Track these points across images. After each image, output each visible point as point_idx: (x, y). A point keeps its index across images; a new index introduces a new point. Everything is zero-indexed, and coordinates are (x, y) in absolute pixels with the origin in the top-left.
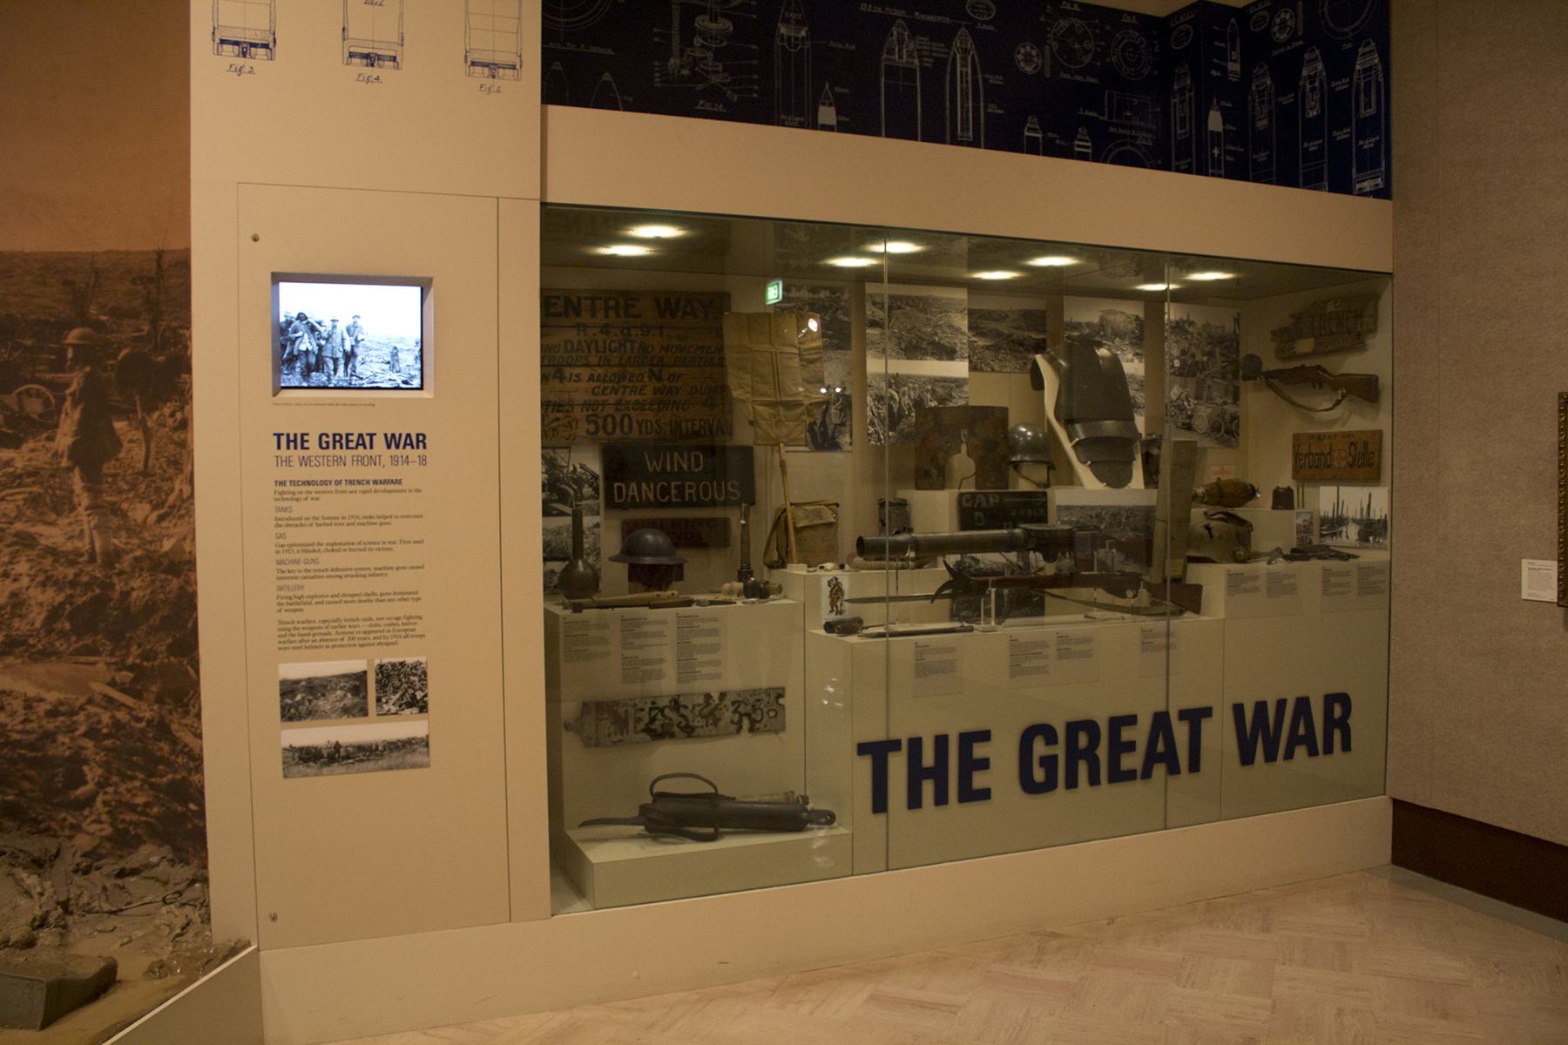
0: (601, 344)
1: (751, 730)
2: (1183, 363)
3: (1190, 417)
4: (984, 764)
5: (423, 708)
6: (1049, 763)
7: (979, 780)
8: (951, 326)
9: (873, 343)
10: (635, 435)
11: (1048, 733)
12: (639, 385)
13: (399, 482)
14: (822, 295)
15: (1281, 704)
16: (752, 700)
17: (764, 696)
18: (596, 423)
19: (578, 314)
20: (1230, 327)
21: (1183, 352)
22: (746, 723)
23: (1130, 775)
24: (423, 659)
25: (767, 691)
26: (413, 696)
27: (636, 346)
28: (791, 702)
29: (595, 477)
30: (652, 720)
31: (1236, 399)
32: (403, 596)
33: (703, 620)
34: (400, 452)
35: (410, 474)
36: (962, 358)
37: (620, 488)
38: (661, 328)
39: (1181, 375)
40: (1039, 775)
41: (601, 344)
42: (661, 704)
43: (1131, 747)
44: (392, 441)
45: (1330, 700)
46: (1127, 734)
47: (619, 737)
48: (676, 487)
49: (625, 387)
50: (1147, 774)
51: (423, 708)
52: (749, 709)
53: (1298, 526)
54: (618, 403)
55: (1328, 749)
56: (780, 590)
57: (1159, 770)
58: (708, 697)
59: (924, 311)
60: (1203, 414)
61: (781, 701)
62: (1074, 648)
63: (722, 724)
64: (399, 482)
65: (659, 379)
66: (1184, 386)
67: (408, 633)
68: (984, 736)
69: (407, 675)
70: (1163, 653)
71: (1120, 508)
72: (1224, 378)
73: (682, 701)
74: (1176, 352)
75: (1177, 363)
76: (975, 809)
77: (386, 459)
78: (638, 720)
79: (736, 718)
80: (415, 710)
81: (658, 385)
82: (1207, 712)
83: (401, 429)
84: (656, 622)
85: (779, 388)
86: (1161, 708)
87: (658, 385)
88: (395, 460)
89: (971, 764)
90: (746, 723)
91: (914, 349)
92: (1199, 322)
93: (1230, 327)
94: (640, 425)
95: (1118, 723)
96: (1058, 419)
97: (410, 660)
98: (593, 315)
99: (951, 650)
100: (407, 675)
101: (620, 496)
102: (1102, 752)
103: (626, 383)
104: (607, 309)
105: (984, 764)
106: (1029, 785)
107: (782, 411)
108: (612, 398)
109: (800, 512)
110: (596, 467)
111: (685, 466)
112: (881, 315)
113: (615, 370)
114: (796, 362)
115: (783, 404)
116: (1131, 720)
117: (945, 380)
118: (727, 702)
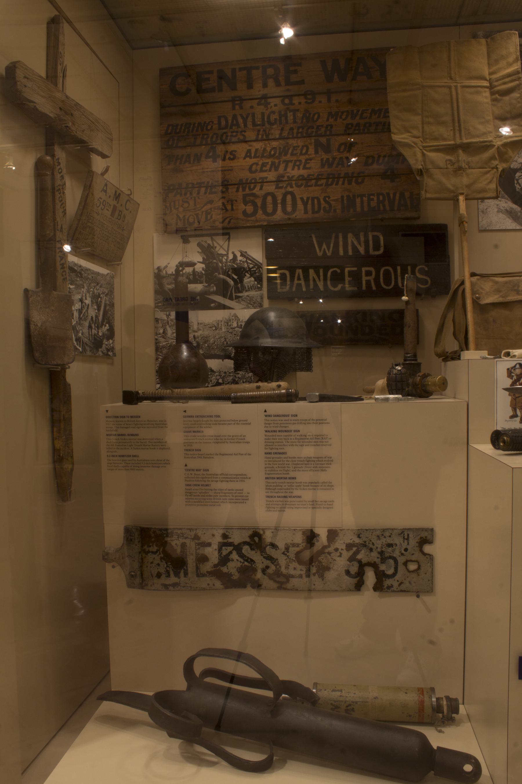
1: (378, 587)
12: (303, 158)
16: (379, 544)
17: (397, 540)
18: (255, 205)
19: (233, 87)
22: (370, 577)
25: (405, 534)
27: (299, 115)
28: (445, 552)
30: (224, 560)
33: (306, 422)
38: (329, 93)
42: (236, 538)
47: (173, 579)
48: (350, 273)
49: (287, 162)
52: (374, 557)
54: (279, 180)
56: (443, 384)
58: (311, 537)
61: (427, 549)
63: (331, 575)
65: (327, 149)
73: (268, 537)
78: (203, 559)
79: (354, 569)
81: (325, 157)
84: (236, 422)
85: (457, 124)
87: (325, 157)
90: (370, 577)
94: (305, 204)
103: (288, 157)
107: (462, 156)
108: (271, 176)
109: (487, 286)
111: (362, 250)
113: (275, 144)
114: (485, 97)
115: (467, 148)
118: (340, 543)
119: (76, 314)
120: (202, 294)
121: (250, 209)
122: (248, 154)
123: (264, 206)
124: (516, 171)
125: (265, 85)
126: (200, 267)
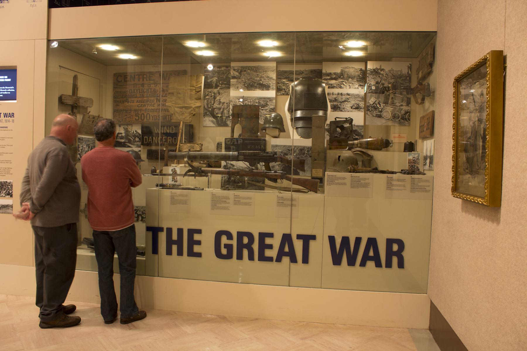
0: (141, 90)
2: (377, 88)
3: (381, 112)
4: (199, 243)
5: (11, 196)
6: (229, 247)
7: (196, 249)
8: (268, 77)
9: (233, 85)
10: (151, 120)
11: (229, 236)
12: (153, 103)
13: (7, 127)
14: (223, 69)
15: (358, 240)
18: (138, 117)
21: (377, 83)
22: (140, 218)
23: (270, 259)
24: (12, 181)
26: (9, 192)
29: (140, 135)
31: (408, 103)
32: (8, 162)
34: (7, 118)
35: (9, 125)
36: (273, 89)
37: (146, 138)
39: (376, 93)
40: (224, 251)
41: (141, 90)
43: (270, 247)
44: (6, 115)
45: (390, 242)
46: (268, 241)
49: (148, 104)
50: (279, 260)
51: (11, 196)
52: (141, 213)
53: (409, 160)
55: (389, 265)
57: (286, 260)
59: (256, 71)
60: (388, 111)
62: (243, 201)
64: (7, 127)
66: (378, 98)
67: (8, 173)
68: (199, 232)
69: (8, 185)
70: (290, 207)
71: (304, 147)
75: (373, 88)
76: (194, 260)
77: (4, 121)
80: (9, 196)
82: (313, 237)
83: (8, 112)
86: (287, 232)
88: (6, 121)
89: (192, 242)
90: (140, 218)
91: (250, 86)
92: (387, 70)
93: (405, 71)
94: (153, 117)
95: (263, 236)
96: (289, 110)
97: (8, 181)
98: (139, 81)
99: (186, 196)
100: (8, 185)
101: (146, 141)
102: (256, 247)
103: (149, 103)
104: (143, 78)
105: (199, 243)
106: (219, 254)
110: (140, 131)
112: (237, 74)
116: (271, 235)
117: (264, 98)
119: (80, 151)
120: (124, 143)
121: (137, 118)
122: (137, 102)
123: (144, 117)
124: (215, 109)
125: (143, 80)
126: (123, 135)
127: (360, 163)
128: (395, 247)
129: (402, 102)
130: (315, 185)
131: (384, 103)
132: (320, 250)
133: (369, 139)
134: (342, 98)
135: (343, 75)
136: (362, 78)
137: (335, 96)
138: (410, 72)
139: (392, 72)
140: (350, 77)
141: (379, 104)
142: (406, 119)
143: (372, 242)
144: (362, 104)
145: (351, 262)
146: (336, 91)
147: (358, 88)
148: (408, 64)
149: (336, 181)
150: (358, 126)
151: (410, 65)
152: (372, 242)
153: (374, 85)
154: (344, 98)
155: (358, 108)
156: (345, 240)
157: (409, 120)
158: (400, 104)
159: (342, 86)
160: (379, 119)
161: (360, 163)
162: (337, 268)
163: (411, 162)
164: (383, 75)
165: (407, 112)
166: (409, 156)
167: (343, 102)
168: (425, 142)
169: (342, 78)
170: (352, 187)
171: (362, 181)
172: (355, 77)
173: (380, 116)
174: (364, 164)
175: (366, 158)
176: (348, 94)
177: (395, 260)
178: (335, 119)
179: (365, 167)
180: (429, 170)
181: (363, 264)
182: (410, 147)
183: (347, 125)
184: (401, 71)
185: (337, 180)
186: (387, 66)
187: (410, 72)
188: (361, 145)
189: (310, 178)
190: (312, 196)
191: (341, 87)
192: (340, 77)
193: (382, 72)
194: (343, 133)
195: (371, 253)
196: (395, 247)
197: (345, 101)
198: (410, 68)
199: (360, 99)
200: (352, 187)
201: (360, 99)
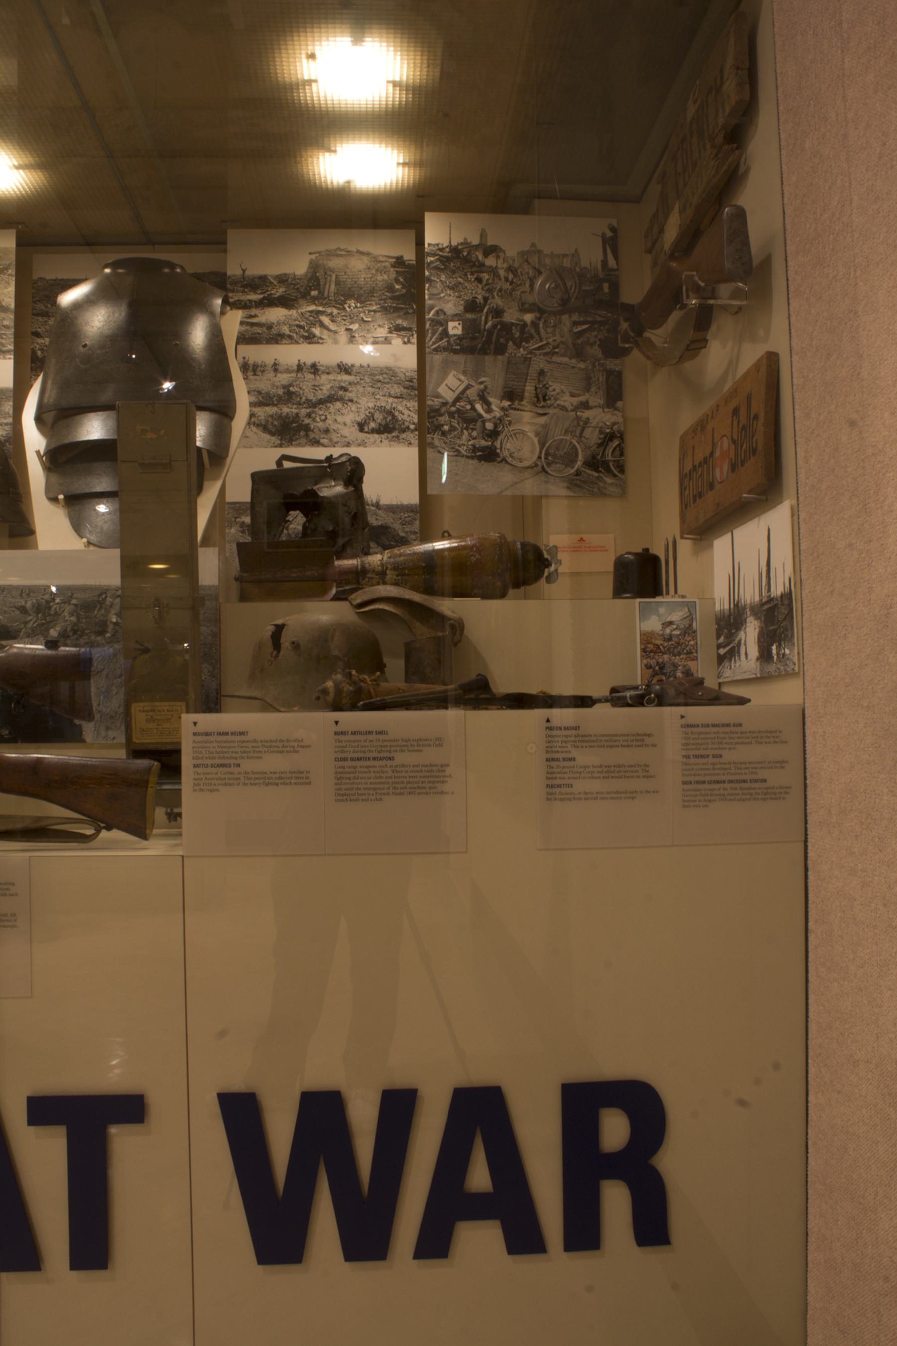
2: (471, 328)
3: (494, 434)
15: (398, 1107)
20: (592, 255)
21: (472, 307)
31: (614, 395)
39: (463, 351)
45: (582, 1103)
53: (647, 638)
55: (583, 1233)
66: (477, 373)
72: (579, 354)
74: (451, 305)
75: (455, 328)
82: (131, 1108)
92: (512, 249)
93: (592, 255)
127: (395, 666)
128: (615, 1130)
129: (587, 389)
130: (136, 794)
131: (503, 398)
132: (176, 1185)
133: (439, 545)
134: (316, 387)
135: (318, 286)
136: (405, 299)
137: (284, 378)
138: (612, 262)
139: (534, 260)
140: (348, 293)
141: (483, 398)
142: (605, 464)
143: (480, 1112)
144: (408, 411)
145: (366, 1240)
146: (291, 354)
147: (387, 341)
148: (602, 226)
149: (248, 766)
150: (392, 509)
151: (613, 229)
152: (480, 1112)
153: (456, 317)
154: (326, 384)
155: (388, 427)
156: (322, 1112)
157: (622, 469)
158: (575, 401)
159: (317, 331)
160: (485, 467)
161: (395, 666)
162: (282, 1277)
163: (657, 650)
164: (493, 271)
165: (611, 437)
166: (644, 616)
167: (321, 402)
168: (721, 544)
169: (314, 300)
170: (347, 789)
171: (401, 758)
172: (372, 291)
173: (489, 455)
174: (414, 670)
175: (422, 632)
176: (344, 369)
177: (616, 1200)
178: (279, 463)
179: (424, 680)
180: (763, 679)
181: (434, 1244)
182: (642, 576)
183: (332, 490)
184: (575, 255)
185: (258, 752)
186: (512, 237)
187: (612, 262)
188: (404, 573)
189: (122, 754)
190: (116, 853)
191: (311, 339)
192: (305, 295)
193: (490, 261)
194: (308, 524)
195: (479, 1177)
196: (615, 1130)
197: (331, 399)
198: (612, 243)
199: (397, 390)
200: (347, 789)
201: (397, 390)
